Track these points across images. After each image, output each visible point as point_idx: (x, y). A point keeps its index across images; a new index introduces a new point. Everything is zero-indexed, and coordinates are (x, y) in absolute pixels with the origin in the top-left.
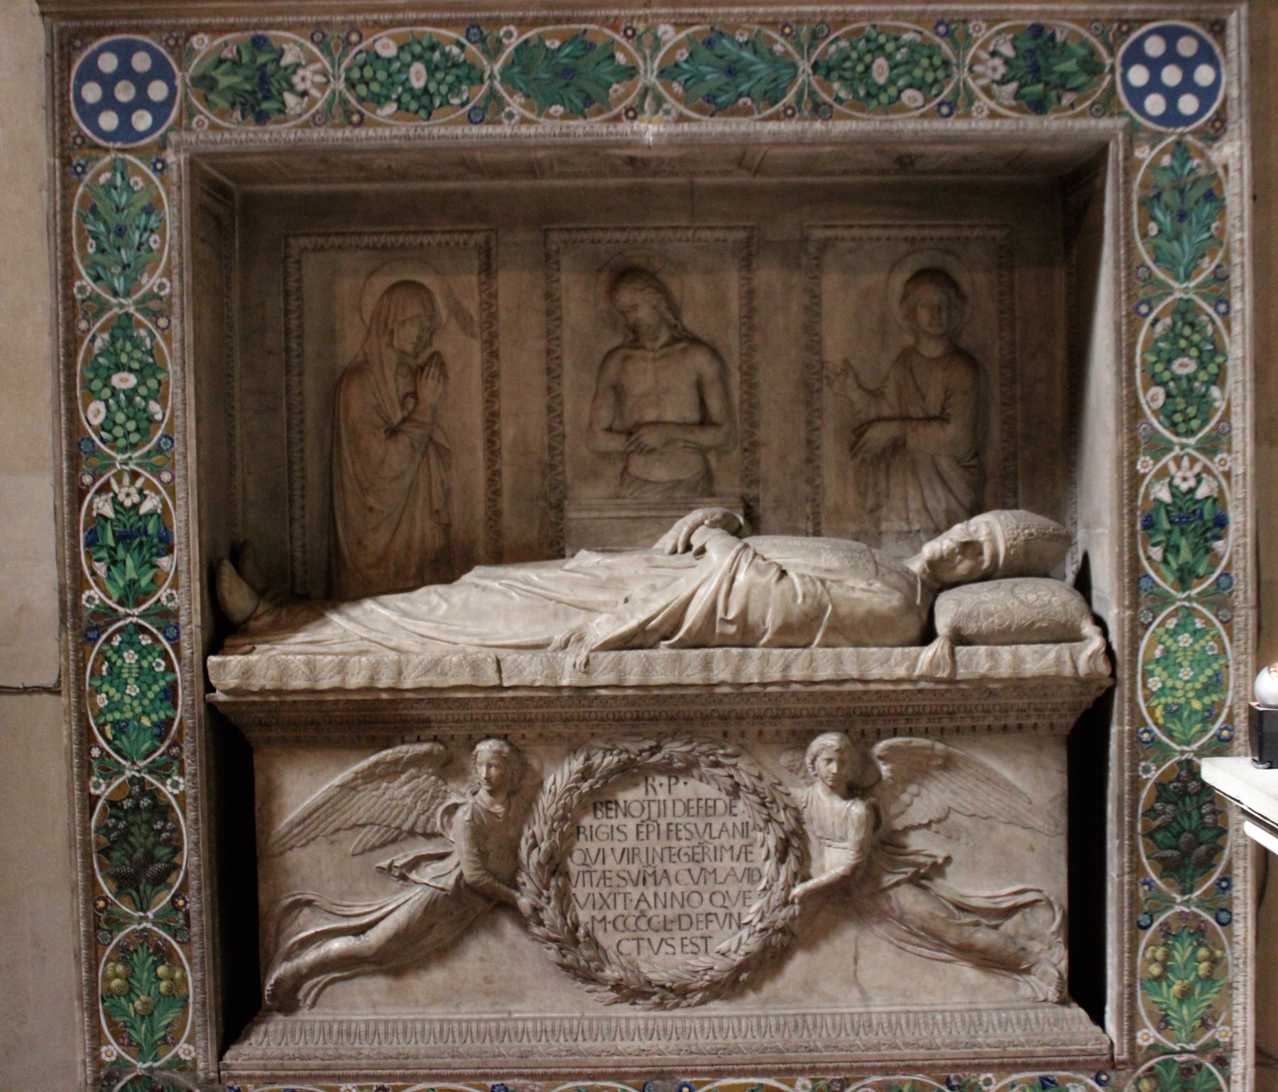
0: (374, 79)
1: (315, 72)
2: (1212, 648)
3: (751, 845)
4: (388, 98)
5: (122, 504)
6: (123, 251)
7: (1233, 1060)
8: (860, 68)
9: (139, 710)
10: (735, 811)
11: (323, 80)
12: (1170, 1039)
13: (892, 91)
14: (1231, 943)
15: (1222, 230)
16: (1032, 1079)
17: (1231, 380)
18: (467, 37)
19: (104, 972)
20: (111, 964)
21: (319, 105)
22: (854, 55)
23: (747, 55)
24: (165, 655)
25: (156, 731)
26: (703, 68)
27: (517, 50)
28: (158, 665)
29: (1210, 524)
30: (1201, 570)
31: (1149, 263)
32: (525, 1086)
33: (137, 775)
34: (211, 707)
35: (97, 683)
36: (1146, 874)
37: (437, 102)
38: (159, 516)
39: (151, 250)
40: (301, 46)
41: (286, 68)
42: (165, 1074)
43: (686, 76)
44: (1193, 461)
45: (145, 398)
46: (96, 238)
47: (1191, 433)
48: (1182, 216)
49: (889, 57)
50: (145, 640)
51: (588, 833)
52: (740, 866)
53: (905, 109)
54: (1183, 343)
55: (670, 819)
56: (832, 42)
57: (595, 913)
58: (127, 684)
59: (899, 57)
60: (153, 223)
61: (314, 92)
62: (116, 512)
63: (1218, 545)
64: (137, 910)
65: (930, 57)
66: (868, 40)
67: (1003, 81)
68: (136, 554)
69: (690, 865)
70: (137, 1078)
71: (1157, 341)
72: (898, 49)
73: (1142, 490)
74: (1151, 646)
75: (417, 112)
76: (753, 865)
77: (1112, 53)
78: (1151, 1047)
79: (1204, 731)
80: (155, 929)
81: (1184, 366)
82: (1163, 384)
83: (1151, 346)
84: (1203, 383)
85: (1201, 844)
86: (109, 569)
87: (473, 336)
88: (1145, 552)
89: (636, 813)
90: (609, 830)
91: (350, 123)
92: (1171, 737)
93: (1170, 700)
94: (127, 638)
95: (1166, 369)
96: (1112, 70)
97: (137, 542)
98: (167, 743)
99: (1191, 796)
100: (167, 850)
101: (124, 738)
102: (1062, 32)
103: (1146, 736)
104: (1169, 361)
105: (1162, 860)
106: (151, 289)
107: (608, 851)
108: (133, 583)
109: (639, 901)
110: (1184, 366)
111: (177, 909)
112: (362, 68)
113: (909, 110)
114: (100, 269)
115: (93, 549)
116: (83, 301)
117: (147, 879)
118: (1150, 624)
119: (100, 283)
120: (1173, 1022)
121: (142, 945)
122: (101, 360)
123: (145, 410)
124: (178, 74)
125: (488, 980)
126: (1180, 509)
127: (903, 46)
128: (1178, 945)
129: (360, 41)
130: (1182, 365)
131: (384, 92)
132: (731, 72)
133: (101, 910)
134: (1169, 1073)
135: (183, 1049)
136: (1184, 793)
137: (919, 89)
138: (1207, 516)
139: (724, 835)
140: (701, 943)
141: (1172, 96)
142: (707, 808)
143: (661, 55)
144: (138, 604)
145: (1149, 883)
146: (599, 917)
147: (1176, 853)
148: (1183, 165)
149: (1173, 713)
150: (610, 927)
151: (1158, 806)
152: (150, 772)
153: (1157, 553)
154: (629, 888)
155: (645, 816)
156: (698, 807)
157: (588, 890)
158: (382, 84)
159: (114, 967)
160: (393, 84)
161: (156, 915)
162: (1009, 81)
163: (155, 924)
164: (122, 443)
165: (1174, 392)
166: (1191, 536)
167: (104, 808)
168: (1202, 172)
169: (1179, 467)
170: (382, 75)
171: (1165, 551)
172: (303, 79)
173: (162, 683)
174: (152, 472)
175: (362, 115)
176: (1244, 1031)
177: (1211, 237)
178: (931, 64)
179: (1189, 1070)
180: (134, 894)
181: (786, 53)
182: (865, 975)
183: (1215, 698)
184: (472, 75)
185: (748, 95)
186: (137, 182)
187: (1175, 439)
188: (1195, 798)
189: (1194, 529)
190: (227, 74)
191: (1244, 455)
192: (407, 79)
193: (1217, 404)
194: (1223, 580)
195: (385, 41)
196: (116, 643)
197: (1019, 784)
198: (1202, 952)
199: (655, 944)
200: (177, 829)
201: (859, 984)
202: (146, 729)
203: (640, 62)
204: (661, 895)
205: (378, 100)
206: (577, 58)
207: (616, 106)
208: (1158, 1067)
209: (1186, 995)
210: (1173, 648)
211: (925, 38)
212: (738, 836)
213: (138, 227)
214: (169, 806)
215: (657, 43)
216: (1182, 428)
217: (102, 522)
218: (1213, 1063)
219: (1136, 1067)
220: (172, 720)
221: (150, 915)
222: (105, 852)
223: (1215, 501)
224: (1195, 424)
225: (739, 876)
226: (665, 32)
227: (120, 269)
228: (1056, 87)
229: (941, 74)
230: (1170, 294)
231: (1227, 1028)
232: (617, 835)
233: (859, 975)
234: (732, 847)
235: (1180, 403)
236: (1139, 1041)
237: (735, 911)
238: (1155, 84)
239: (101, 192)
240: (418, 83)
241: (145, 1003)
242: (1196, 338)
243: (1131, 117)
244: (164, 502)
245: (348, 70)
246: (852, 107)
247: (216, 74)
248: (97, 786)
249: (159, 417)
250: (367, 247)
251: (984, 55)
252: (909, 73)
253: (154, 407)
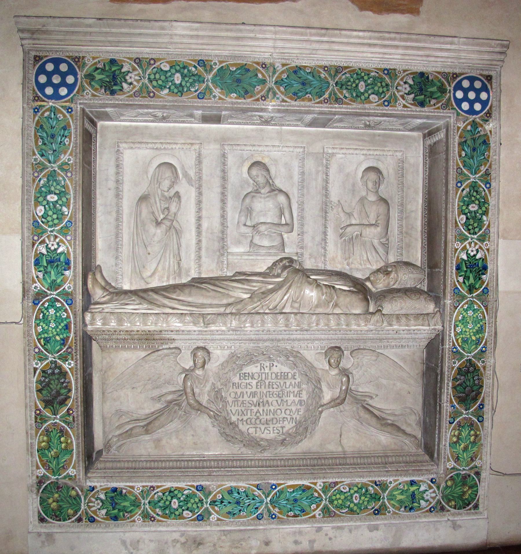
0: (160, 79)
1: (135, 75)
2: (480, 316)
3: (301, 391)
4: (165, 87)
5: (50, 249)
6: (53, 144)
8: (354, 85)
9: (55, 333)
10: (295, 377)
11: (139, 78)
12: (459, 465)
13: (366, 95)
14: (483, 429)
15: (489, 156)
16: (407, 481)
17: (490, 214)
18: (198, 64)
19: (39, 439)
20: (42, 436)
21: (136, 89)
22: (352, 80)
23: (310, 77)
24: (66, 311)
25: (62, 342)
26: (293, 82)
27: (218, 70)
28: (64, 315)
30: (477, 286)
31: (462, 167)
32: (210, 485)
33: (54, 360)
34: (85, 333)
35: (38, 322)
36: (453, 402)
37: (185, 90)
38: (65, 254)
39: (65, 144)
40: (130, 64)
41: (124, 73)
42: (64, 481)
43: (286, 85)
44: (476, 244)
45: (60, 205)
46: (42, 139)
47: (475, 233)
48: (474, 149)
49: (365, 81)
50: (58, 305)
51: (237, 385)
52: (297, 399)
53: (371, 102)
54: (473, 199)
55: (269, 380)
56: (343, 74)
57: (239, 417)
58: (50, 322)
59: (369, 82)
60: (66, 133)
61: (135, 83)
62: (48, 252)
63: (484, 277)
64: (53, 415)
65: (381, 83)
66: (357, 74)
67: (408, 94)
68: (55, 269)
69: (277, 399)
70: (52, 482)
71: (464, 197)
72: (369, 78)
74: (457, 316)
75: (177, 93)
76: (302, 399)
77: (450, 86)
78: (452, 469)
79: (476, 348)
80: (60, 422)
81: (473, 207)
82: (466, 214)
83: (462, 199)
84: (480, 214)
85: (473, 391)
86: (44, 275)
87: (192, 186)
89: (256, 378)
90: (245, 384)
91: (149, 96)
92: (464, 350)
93: (464, 336)
94: (51, 304)
95: (467, 208)
96: (450, 92)
97: (56, 264)
98: (67, 347)
99: (470, 373)
100: (66, 390)
101: (48, 344)
102: (431, 76)
103: (455, 350)
104: (468, 205)
105: (459, 397)
106: (65, 160)
107: (245, 392)
108: (54, 281)
109: (257, 412)
110: (473, 207)
111: (69, 415)
112: (155, 74)
113: (372, 102)
114: (43, 152)
115: (38, 267)
116: (36, 164)
117: (57, 403)
118: (458, 306)
119: (43, 157)
121: (55, 429)
122: (43, 189)
123: (61, 210)
124: (79, 73)
125: (195, 443)
127: (371, 77)
128: (463, 430)
129: (154, 64)
130: (473, 207)
131: (164, 84)
132: (303, 84)
133: (37, 415)
134: (458, 479)
135: (71, 471)
136: (468, 372)
137: (377, 95)
138: (480, 266)
139: (291, 387)
140: (280, 429)
141: (472, 103)
142: (284, 376)
143: (276, 76)
144: (56, 290)
145: (453, 406)
146: (240, 419)
147: (464, 394)
148: (475, 130)
149: (465, 341)
150: (245, 423)
151: (458, 377)
152: (59, 359)
153: (461, 279)
154: (253, 408)
155: (260, 379)
156: (281, 376)
157: (236, 408)
158: (163, 82)
159: (43, 438)
160: (167, 81)
161: (61, 417)
162: (411, 94)
163: (60, 421)
164: (51, 223)
165: (469, 217)
166: (474, 273)
167: (40, 373)
168: (482, 133)
169: (470, 246)
170: (163, 78)
171: (464, 278)
172: (131, 78)
173: (65, 322)
174: (63, 236)
175: (154, 93)
177: (485, 158)
178: (382, 85)
179: (466, 477)
180: (52, 408)
181: (326, 77)
182: (344, 441)
183: (480, 335)
184: (200, 79)
185: (310, 94)
186: (60, 116)
188: (472, 374)
190: (99, 74)
192: (173, 80)
193: (485, 223)
194: (485, 290)
195: (165, 64)
196: (46, 306)
197: (406, 368)
198: (472, 432)
199: (263, 429)
200: (70, 382)
201: (341, 445)
202: (57, 341)
203: (268, 78)
204: (265, 410)
205: (162, 87)
206: (242, 75)
207: (257, 95)
209: (465, 449)
210: (466, 316)
211: (380, 75)
212: (296, 387)
213: (60, 135)
214: (67, 372)
215: (275, 71)
216: (472, 231)
217: (42, 256)
218: (474, 474)
220: (69, 337)
221: (58, 417)
222: (39, 391)
223: (483, 259)
224: (477, 230)
225: (297, 403)
226: (278, 67)
227: (52, 152)
228: (428, 97)
229: (385, 89)
230: (470, 179)
232: (249, 386)
233: (342, 441)
234: (294, 392)
235: (471, 222)
237: (294, 417)
238: (465, 98)
239: (45, 120)
240: (178, 82)
241: (55, 453)
242: (478, 197)
243: (457, 111)
244: (67, 248)
245: (149, 75)
246: (351, 100)
247: (95, 74)
248: (37, 364)
249: (66, 213)
250: (150, 148)
251: (402, 83)
252: (373, 88)
253: (65, 209)
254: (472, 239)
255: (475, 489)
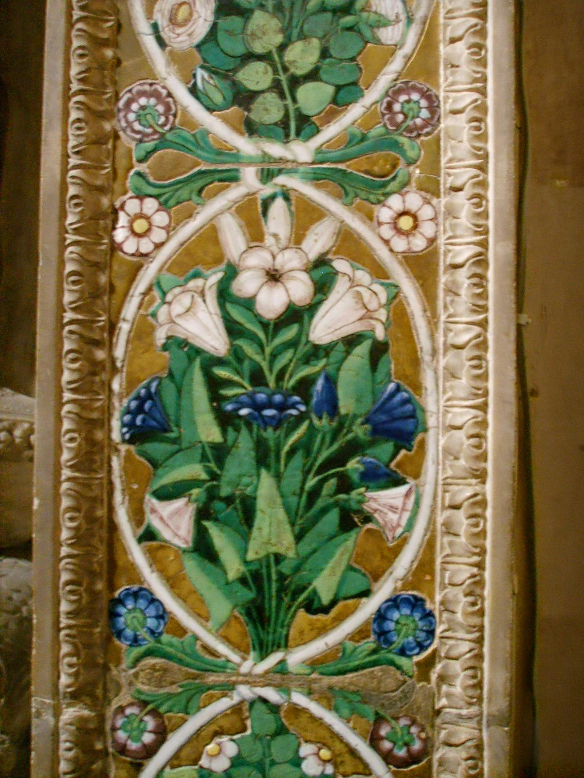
29: (360, 431)
73: (130, 310)
88: (138, 515)
118: (150, 751)
126: (257, 378)
166: (293, 471)
171: (203, 514)
187: (245, 145)
189: (305, 446)
191: (479, 199)
193: (388, 35)
254: (267, 176)
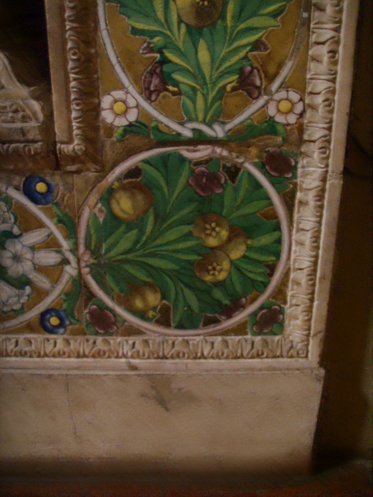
7: (302, 162)
78: (130, 128)
120: (177, 77)
176: (329, 102)
179: (213, 178)
208: (147, 168)
218: (262, 167)
219: (104, 171)
231: (294, 96)
236: (107, 116)
255: (265, 240)
